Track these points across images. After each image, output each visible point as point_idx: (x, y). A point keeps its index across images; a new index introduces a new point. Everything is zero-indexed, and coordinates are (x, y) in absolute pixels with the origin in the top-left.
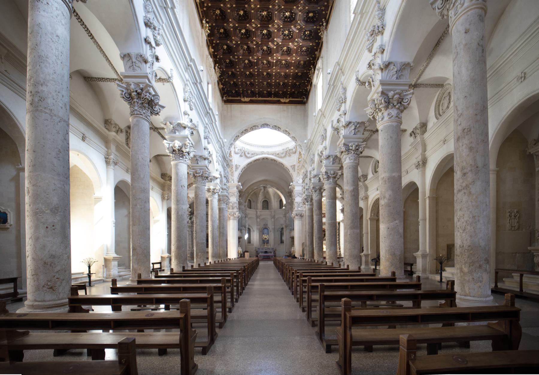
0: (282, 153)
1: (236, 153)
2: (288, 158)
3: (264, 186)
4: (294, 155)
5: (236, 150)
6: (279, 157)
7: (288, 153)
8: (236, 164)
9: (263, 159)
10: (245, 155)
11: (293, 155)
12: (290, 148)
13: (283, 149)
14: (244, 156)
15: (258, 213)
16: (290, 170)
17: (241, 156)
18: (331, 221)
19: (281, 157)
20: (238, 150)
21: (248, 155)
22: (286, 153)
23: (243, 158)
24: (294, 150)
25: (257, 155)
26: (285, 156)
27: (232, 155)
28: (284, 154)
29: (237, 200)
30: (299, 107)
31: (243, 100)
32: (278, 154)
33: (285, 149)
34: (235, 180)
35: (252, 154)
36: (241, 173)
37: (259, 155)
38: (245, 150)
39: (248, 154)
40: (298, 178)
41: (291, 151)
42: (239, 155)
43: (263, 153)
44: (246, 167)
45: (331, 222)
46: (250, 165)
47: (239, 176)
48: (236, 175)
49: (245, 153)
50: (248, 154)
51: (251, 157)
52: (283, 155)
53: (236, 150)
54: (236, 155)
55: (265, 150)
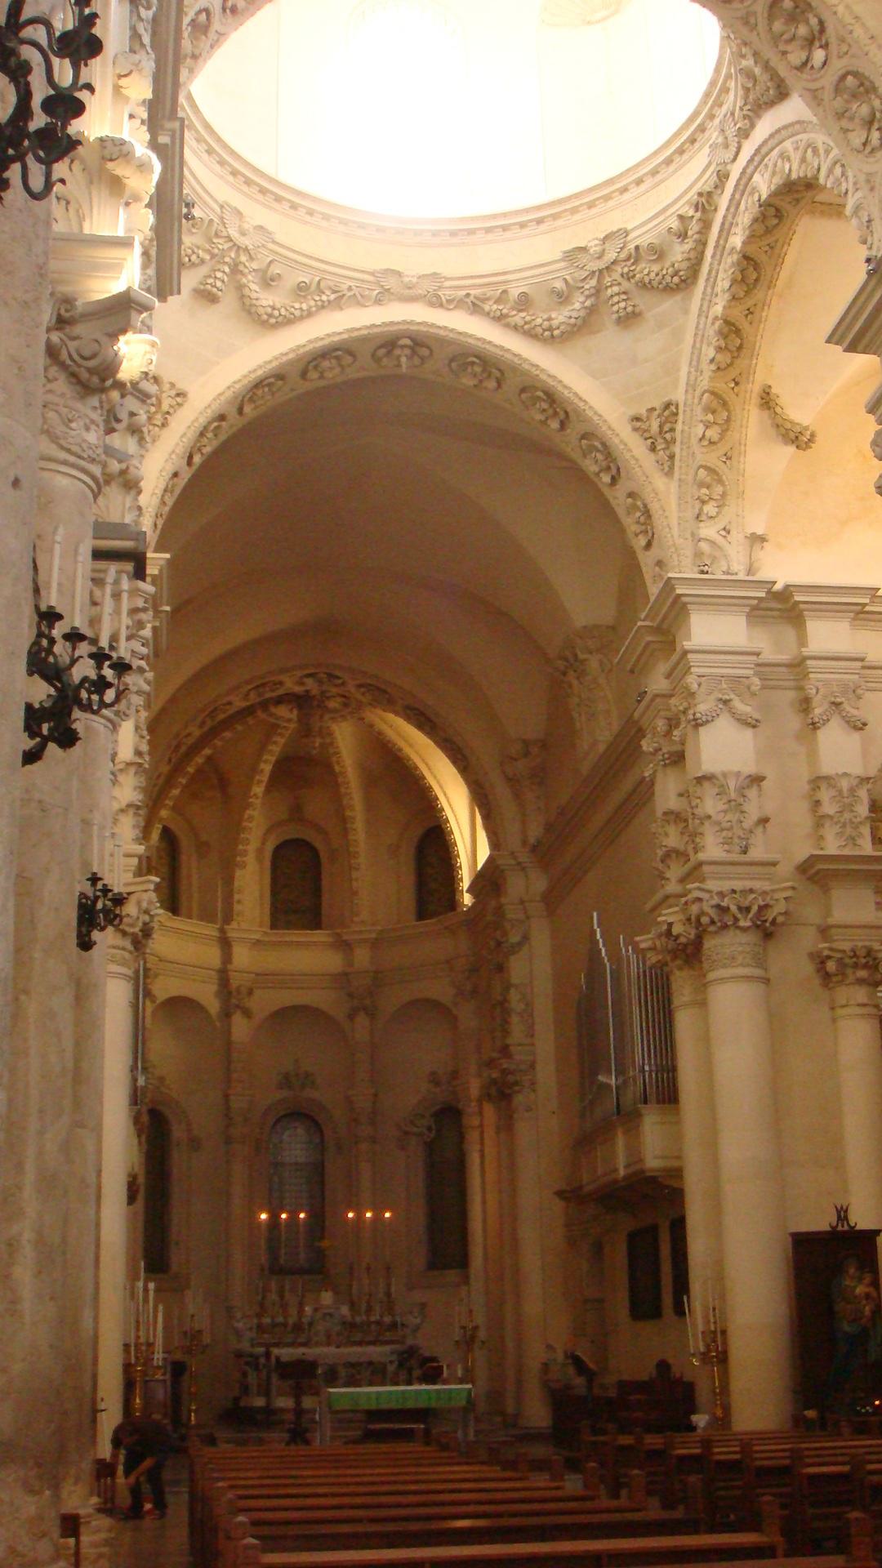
0: (563, 298)
2: (609, 340)
4: (669, 304)
6: (530, 333)
9: (388, 343)
13: (573, 255)
19: (548, 337)
22: (598, 291)
25: (339, 301)
28: (578, 303)
32: (524, 302)
33: (595, 249)
35: (301, 290)
37: (359, 301)
44: (232, 412)
51: (289, 321)
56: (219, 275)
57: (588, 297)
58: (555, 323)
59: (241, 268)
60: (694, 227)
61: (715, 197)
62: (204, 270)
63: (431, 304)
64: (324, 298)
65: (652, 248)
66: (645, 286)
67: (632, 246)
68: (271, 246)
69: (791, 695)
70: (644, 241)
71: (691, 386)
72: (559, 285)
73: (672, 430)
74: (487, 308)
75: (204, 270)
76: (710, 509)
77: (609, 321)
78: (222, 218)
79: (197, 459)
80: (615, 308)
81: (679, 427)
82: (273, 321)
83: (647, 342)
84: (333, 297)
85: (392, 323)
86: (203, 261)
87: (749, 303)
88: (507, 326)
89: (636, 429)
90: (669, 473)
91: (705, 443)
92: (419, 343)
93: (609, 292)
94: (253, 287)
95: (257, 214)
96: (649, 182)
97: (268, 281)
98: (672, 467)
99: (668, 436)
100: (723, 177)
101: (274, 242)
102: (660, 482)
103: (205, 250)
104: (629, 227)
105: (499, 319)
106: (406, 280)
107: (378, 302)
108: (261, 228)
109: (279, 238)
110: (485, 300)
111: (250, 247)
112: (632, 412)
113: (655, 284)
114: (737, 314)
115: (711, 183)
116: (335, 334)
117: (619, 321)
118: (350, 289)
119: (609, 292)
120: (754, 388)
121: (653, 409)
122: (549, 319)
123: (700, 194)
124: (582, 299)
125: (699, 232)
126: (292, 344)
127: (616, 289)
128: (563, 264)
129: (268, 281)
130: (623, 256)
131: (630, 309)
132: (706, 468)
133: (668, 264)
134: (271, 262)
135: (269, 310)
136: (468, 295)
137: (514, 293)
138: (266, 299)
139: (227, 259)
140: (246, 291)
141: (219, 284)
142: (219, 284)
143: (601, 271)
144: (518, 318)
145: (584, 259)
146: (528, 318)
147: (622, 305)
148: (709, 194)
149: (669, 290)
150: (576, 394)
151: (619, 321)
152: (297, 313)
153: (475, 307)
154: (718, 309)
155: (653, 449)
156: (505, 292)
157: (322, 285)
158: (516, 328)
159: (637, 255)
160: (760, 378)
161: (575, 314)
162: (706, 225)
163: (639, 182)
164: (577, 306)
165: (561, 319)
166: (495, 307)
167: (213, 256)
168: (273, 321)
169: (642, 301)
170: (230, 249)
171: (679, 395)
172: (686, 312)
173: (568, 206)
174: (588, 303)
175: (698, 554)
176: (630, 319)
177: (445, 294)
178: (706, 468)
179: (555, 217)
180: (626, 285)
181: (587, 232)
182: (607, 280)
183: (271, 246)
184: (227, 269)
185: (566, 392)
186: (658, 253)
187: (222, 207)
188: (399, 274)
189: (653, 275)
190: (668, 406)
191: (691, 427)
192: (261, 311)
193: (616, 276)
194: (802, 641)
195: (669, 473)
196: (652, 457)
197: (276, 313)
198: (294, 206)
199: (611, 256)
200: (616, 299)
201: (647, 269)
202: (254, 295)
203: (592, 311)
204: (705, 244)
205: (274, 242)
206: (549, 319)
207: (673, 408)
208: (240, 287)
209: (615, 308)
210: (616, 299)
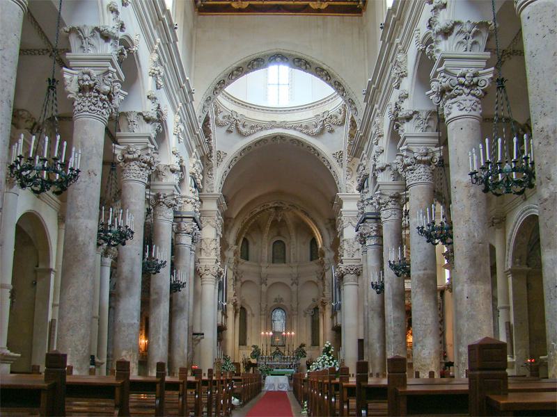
1: (219, 125)
2: (327, 135)
3: (276, 205)
5: (220, 117)
6: (308, 134)
7: (325, 127)
8: (217, 150)
9: (275, 137)
10: (238, 129)
11: (337, 129)
15: (264, 270)
16: (331, 164)
17: (229, 131)
18: (422, 272)
20: (224, 117)
21: (244, 130)
22: (323, 125)
23: (234, 136)
25: (261, 130)
26: (321, 132)
27: (211, 128)
29: (217, 234)
30: (349, 18)
31: (234, 5)
32: (307, 127)
34: (215, 185)
35: (252, 127)
36: (229, 170)
37: (266, 129)
38: (238, 118)
39: (244, 126)
40: (349, 182)
42: (226, 128)
45: (424, 274)
46: (247, 152)
47: (225, 177)
48: (219, 174)
49: (237, 125)
50: (244, 126)
51: (250, 135)
52: (315, 130)
53: (220, 117)
55: (279, 118)
70: (333, 114)
79: (231, 167)
92: (282, 137)
95: (241, 111)
109: (246, 116)
137: (303, 125)
149: (341, 125)
153: (295, 129)
163: (332, 99)
171: (342, 150)
176: (331, 131)
181: (319, 111)
201: (334, 120)
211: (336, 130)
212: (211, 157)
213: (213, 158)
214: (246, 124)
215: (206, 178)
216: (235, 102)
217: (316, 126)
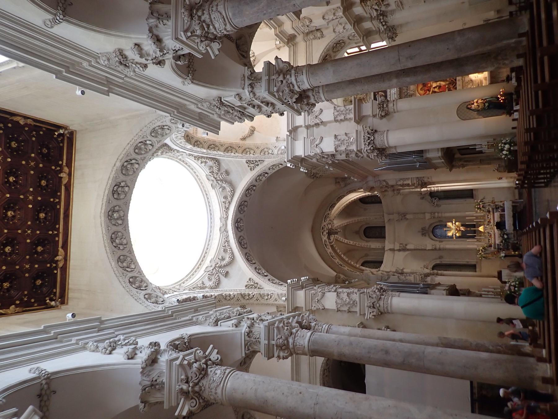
0: (224, 188)
2: (233, 177)
6: (233, 196)
12: (208, 172)
14: (227, 269)
22: (221, 181)
23: (232, 271)
24: (210, 163)
25: (228, 242)
26: (231, 184)
32: (225, 197)
33: (211, 182)
35: (225, 251)
41: (215, 170)
43: (223, 229)
44: (254, 266)
49: (220, 267)
51: (232, 253)
52: (228, 189)
54: (221, 286)
55: (218, 223)
56: (221, 272)
57: (223, 183)
58: (230, 190)
59: (220, 266)
60: (203, 160)
61: (195, 156)
62: (220, 275)
63: (227, 219)
64: (227, 245)
65: (210, 169)
66: (219, 170)
67: (210, 174)
68: (215, 259)
69: (314, 128)
70: (209, 171)
71: (242, 158)
72: (221, 189)
73: (253, 161)
74: (227, 206)
75: (220, 275)
76: (270, 151)
77: (229, 178)
78: (208, 271)
79: (266, 274)
80: (225, 176)
81: (252, 160)
82: (232, 257)
83: (233, 168)
84: (226, 243)
85: (232, 229)
86: (218, 276)
87: (220, 146)
88: (231, 201)
89: (254, 170)
90: (263, 161)
91: (254, 154)
93: (221, 178)
94: (224, 263)
95: (207, 263)
96: (195, 170)
97: (223, 259)
98: (262, 160)
99: (254, 162)
100: (190, 155)
101: (214, 258)
102: (265, 163)
103: (216, 275)
104: (205, 175)
105: (230, 203)
106: (222, 226)
107: (227, 232)
108: (210, 262)
109: (213, 257)
110: (226, 207)
111: (215, 264)
112: (249, 170)
113: (218, 168)
114: (223, 148)
115: (192, 157)
116: (235, 242)
117: (228, 175)
118: (224, 239)
119: (221, 178)
120: (241, 142)
121: (248, 166)
122: (229, 191)
123: (195, 159)
124: (223, 184)
125: (204, 159)
126: (238, 252)
127: (220, 176)
128: (216, 189)
129: (223, 259)
130: (212, 176)
131: (225, 173)
132: (260, 153)
133: (213, 165)
134: (218, 259)
135: (230, 258)
136: (225, 211)
137: (224, 200)
138: (227, 260)
139: (218, 270)
140: (225, 264)
141: (224, 271)
142: (224, 271)
143: (216, 180)
144: (229, 199)
145: (214, 184)
146: (229, 196)
147: (224, 175)
148: (195, 157)
150: (246, 184)
151: (228, 175)
152: (230, 251)
153: (228, 209)
154: (222, 153)
155: (258, 165)
156: (223, 202)
157: (224, 245)
158: (232, 199)
159: (212, 172)
160: (238, 141)
161: (227, 186)
162: (202, 157)
163: (195, 172)
164: (225, 185)
165: (229, 189)
166: (227, 204)
167: (217, 273)
168: (232, 257)
169: (222, 170)
170: (215, 269)
172: (224, 160)
173: (202, 188)
174: (224, 183)
175: (281, 154)
176: (227, 173)
177: (225, 216)
178: (260, 153)
179: (205, 191)
180: (219, 174)
181: (208, 184)
182: (218, 179)
183: (215, 259)
184: (220, 270)
185: (246, 186)
186: (211, 167)
187: (205, 272)
188: (220, 227)
189: (216, 168)
190: (247, 163)
191: (251, 157)
192: (230, 260)
193: (217, 177)
194: (301, 126)
195: (263, 161)
196: (260, 165)
197: (230, 257)
198: (206, 253)
199: (213, 178)
200: (223, 176)
202: (226, 262)
203: (226, 182)
204: (207, 157)
205: (214, 258)
206: (229, 191)
207: (247, 161)
208: (225, 266)
209: (225, 176)
210: (223, 176)
211: (226, 168)
212: (249, 295)
213: (250, 293)
214: (220, 257)
215: (271, 301)
216: (198, 268)
217: (224, 188)
